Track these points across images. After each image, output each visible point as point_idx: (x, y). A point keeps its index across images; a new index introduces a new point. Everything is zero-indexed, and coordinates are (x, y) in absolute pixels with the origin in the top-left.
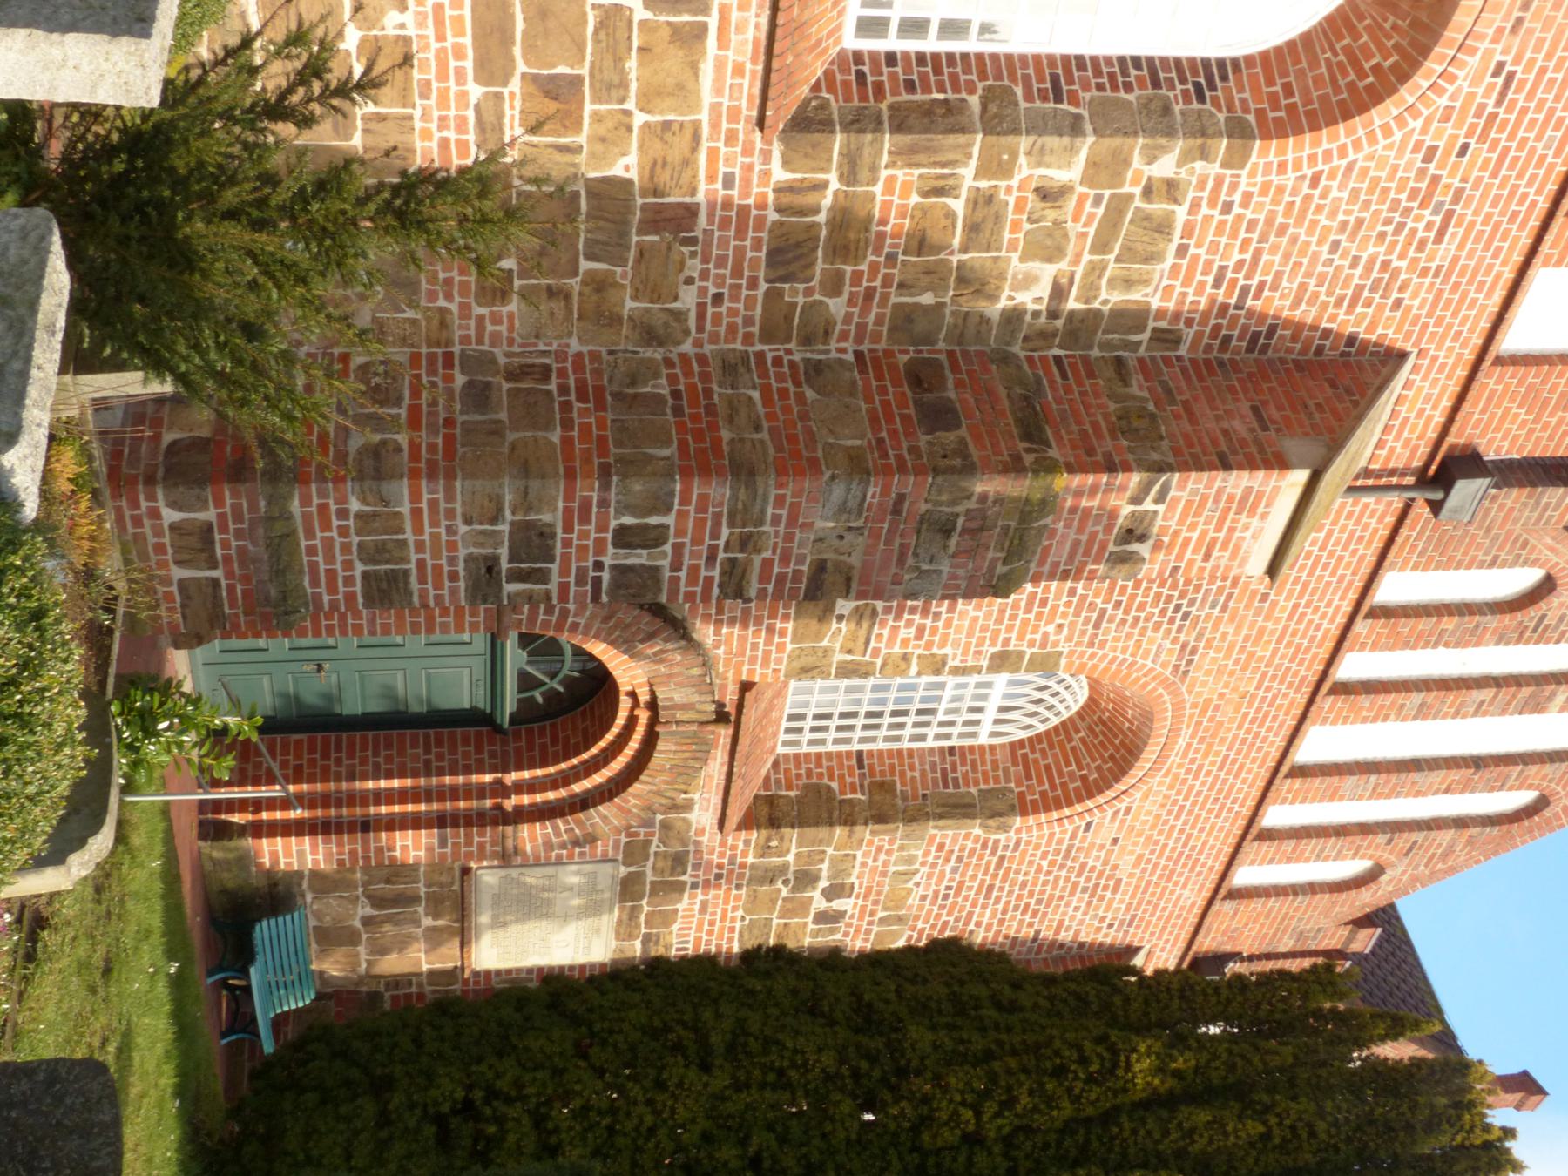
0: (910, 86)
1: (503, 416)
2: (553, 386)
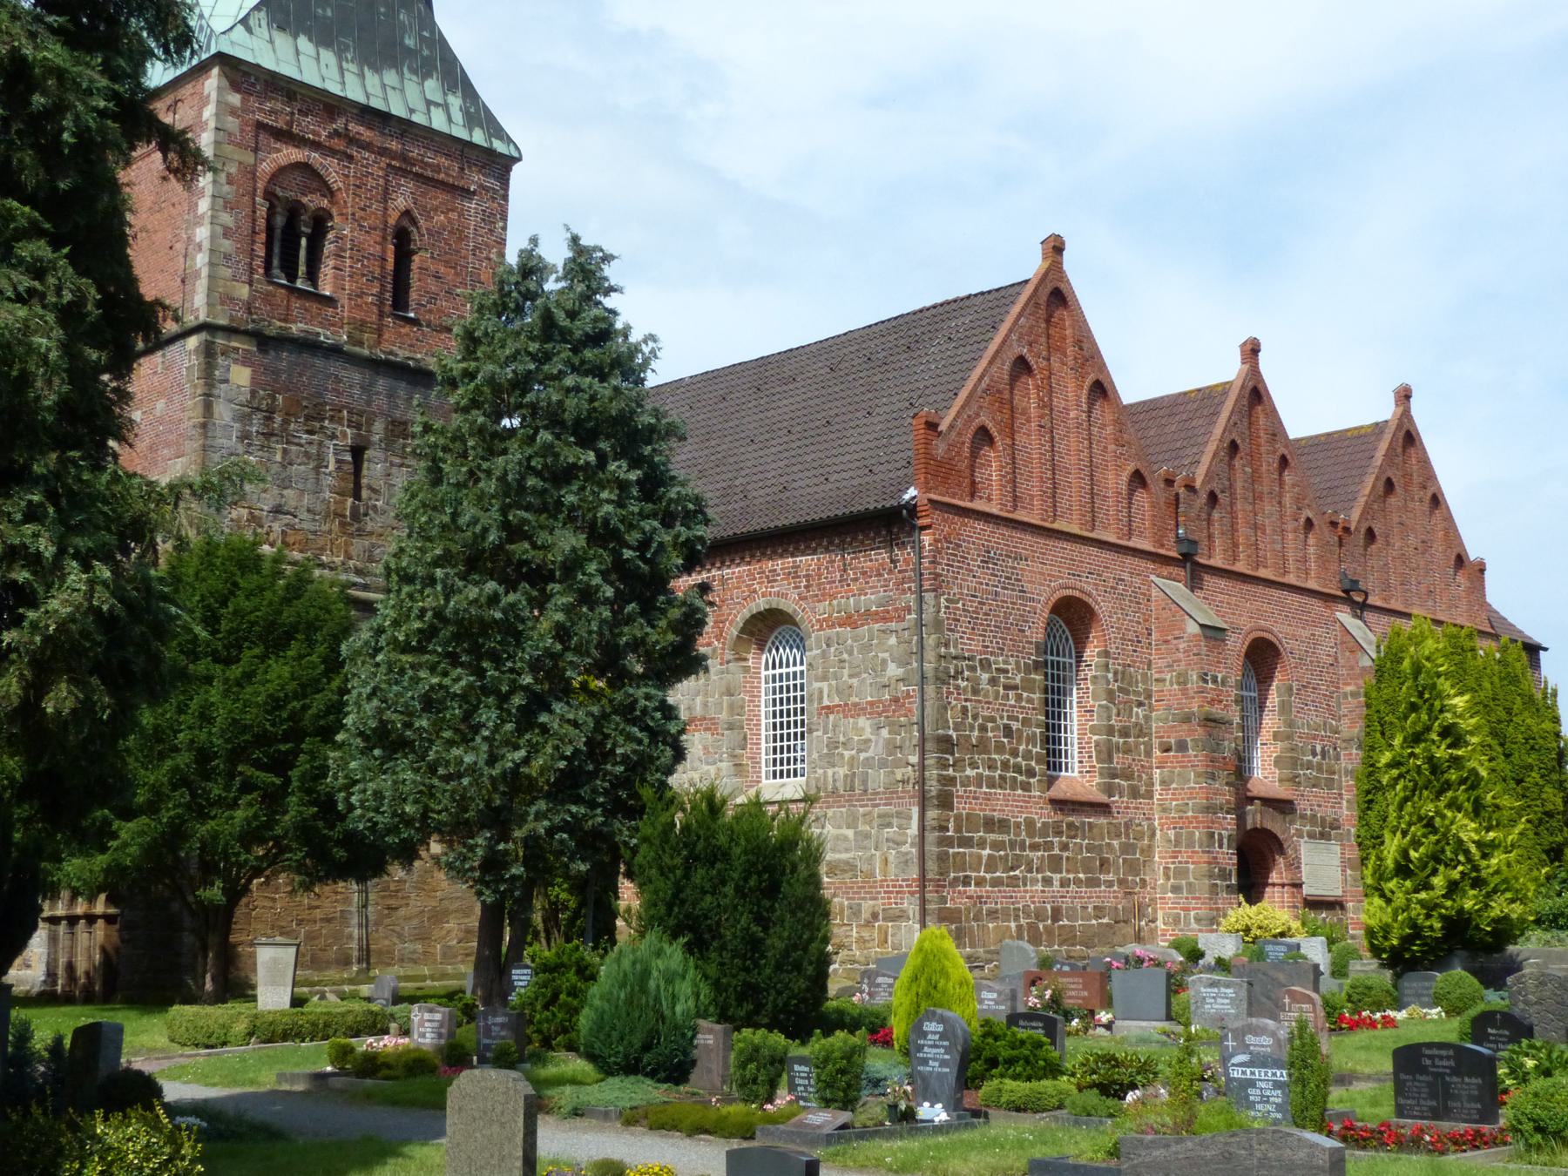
0: (1090, 757)
1: (1184, 882)
2: (1172, 866)
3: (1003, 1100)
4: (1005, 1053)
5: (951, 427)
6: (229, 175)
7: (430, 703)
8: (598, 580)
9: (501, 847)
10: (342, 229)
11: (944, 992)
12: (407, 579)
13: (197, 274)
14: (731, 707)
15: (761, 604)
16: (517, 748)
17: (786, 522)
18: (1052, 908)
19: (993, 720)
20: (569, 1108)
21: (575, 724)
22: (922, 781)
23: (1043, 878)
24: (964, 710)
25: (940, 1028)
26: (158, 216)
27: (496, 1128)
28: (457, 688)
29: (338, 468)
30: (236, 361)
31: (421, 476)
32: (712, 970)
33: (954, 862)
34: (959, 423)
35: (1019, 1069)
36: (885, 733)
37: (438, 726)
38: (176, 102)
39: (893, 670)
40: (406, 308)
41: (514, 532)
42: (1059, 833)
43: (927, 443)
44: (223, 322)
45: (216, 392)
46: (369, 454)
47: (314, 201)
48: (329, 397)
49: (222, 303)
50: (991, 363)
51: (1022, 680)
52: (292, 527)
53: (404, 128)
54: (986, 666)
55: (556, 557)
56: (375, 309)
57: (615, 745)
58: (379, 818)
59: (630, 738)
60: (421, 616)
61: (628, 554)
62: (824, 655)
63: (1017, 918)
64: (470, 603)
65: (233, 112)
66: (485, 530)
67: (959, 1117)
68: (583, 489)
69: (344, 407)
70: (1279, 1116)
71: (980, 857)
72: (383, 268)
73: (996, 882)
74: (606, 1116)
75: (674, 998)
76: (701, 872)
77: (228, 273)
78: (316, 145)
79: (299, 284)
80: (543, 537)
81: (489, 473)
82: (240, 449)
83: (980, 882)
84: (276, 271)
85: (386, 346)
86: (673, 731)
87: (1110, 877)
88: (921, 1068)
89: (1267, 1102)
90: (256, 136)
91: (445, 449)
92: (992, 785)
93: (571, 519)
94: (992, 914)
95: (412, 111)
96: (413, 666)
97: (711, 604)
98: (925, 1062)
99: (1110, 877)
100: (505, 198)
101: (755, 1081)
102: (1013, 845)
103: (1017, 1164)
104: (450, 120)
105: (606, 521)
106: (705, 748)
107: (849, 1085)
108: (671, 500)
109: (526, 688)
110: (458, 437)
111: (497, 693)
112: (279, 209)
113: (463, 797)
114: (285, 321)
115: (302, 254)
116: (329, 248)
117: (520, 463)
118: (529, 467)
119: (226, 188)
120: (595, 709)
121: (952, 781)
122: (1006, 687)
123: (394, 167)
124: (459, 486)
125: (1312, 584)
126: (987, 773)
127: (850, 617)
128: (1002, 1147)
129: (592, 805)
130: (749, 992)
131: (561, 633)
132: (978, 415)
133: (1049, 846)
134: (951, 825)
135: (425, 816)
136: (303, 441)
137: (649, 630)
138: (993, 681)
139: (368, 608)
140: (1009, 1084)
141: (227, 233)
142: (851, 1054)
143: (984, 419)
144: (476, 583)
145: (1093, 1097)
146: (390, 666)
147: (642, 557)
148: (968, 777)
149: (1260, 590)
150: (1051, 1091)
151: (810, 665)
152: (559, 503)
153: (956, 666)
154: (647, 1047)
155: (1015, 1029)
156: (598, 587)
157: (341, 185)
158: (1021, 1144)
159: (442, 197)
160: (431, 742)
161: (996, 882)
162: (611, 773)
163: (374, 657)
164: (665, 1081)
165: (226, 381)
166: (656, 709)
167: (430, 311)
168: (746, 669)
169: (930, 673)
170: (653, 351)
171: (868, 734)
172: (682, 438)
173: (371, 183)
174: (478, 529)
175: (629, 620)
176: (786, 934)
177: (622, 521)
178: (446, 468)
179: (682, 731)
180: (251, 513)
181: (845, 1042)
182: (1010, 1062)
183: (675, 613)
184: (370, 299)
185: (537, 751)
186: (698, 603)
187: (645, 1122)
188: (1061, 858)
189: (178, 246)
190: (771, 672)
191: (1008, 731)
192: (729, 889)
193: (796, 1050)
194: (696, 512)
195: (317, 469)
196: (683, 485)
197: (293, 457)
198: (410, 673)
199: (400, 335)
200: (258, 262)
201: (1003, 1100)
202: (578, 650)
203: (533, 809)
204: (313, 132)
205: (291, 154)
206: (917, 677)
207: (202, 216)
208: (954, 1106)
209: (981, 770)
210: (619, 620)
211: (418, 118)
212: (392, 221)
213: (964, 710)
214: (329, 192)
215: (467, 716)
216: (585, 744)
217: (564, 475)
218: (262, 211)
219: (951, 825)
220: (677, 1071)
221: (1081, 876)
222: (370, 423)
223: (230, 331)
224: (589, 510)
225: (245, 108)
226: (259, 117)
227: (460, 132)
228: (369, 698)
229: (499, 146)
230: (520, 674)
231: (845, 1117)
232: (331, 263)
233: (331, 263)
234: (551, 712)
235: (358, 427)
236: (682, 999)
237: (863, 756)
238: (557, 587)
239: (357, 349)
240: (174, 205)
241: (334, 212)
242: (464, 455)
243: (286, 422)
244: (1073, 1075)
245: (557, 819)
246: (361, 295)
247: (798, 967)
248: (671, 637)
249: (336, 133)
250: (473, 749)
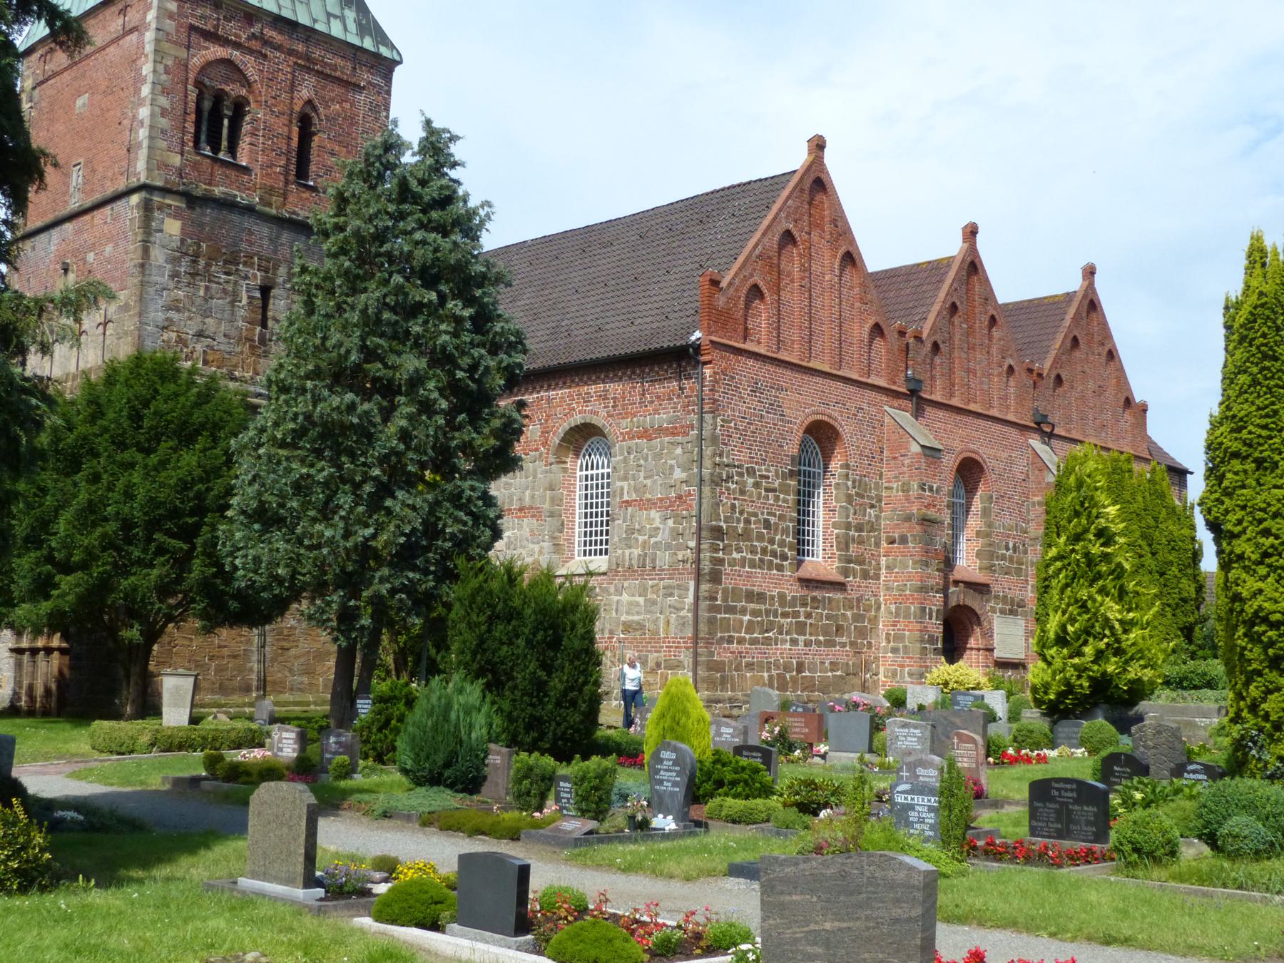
3: (723, 813)
4: (729, 776)
5: (730, 284)
6: (166, 66)
7: (300, 487)
8: (435, 395)
9: (352, 603)
10: (257, 113)
11: (684, 727)
12: (284, 389)
13: (139, 145)
14: (553, 499)
15: (578, 419)
16: (367, 526)
17: (599, 356)
18: (797, 663)
19: (755, 515)
20: (380, 811)
21: (413, 508)
22: (698, 561)
23: (791, 639)
24: (733, 507)
25: (673, 756)
26: (110, 97)
27: (285, 830)
28: (320, 477)
29: (250, 303)
30: (169, 215)
31: (299, 308)
32: (506, 705)
33: (721, 625)
34: (737, 281)
35: (739, 789)
36: (670, 523)
37: (305, 505)
38: (126, 7)
39: (679, 474)
40: (306, 178)
41: (370, 354)
42: (804, 605)
43: (711, 296)
44: (159, 183)
45: (152, 239)
46: (274, 292)
47: (234, 89)
48: (243, 245)
50: (764, 234)
51: (780, 484)
52: (211, 348)
53: (309, 34)
54: (751, 472)
55: (402, 376)
56: (282, 178)
57: (445, 526)
58: (257, 578)
59: (457, 520)
60: (294, 419)
61: (460, 374)
62: (625, 460)
63: (769, 669)
64: (333, 410)
65: (171, 16)
66: (348, 352)
67: (685, 827)
68: (426, 322)
69: (255, 254)
70: (931, 833)
71: (741, 622)
72: (288, 145)
73: (754, 642)
74: (408, 818)
75: (471, 726)
76: (501, 627)
77: (164, 144)
78: (237, 45)
79: (221, 156)
80: (392, 359)
81: (353, 307)
82: (171, 285)
83: (741, 641)
84: (203, 145)
85: (289, 207)
86: (492, 515)
87: (844, 639)
88: (657, 787)
89: (923, 822)
90: (189, 37)
91: (318, 287)
92: (753, 565)
93: (417, 345)
94: (750, 666)
95: (315, 21)
96: (287, 459)
97: (527, 416)
98: (661, 782)
99: (844, 639)
100: (389, 93)
101: (528, 793)
102: (768, 612)
103: (720, 867)
104: (345, 29)
105: (444, 348)
106: (532, 531)
107: (601, 799)
108: (496, 333)
109: (375, 479)
110: (328, 278)
111: (353, 482)
112: (206, 96)
113: (323, 564)
114: (210, 184)
115: (225, 132)
116: (246, 128)
117: (378, 300)
118: (386, 304)
119: (164, 77)
120: (430, 497)
121: (721, 561)
122: (767, 490)
123: (299, 65)
124: (327, 316)
125: (1011, 417)
126: (749, 556)
127: (646, 431)
128: (710, 853)
129: (426, 572)
130: (534, 723)
131: (405, 436)
132: (752, 276)
133: (796, 614)
134: (719, 597)
135: (295, 573)
136: (222, 281)
137: (474, 435)
138: (757, 485)
139: (254, 409)
140: (730, 801)
142: (602, 775)
143: (757, 279)
144: (339, 394)
145: (793, 813)
146: (270, 458)
147: (471, 378)
148: (735, 559)
149: (970, 420)
150: (761, 807)
151: (615, 468)
152: (407, 333)
153: (728, 472)
154: (447, 765)
155: (738, 758)
156: (435, 401)
157: (257, 78)
158: (726, 850)
159: (337, 90)
160: (299, 518)
161: (754, 642)
162: (442, 548)
163: (256, 450)
164: (462, 791)
165: (161, 231)
166: (479, 498)
168: (565, 470)
169: (706, 477)
170: (488, 215)
171: (657, 523)
172: (509, 285)
173: (281, 77)
174: (343, 351)
175: (459, 428)
176: (565, 678)
177: (456, 348)
178: (318, 301)
179: (500, 517)
180: (179, 336)
181: (599, 765)
182: (733, 783)
183: (496, 423)
184: (278, 170)
185: (383, 529)
186: (515, 415)
187: (436, 825)
188: (806, 624)
189: (126, 122)
190: (584, 473)
191: (767, 524)
192: (521, 642)
193: (563, 770)
194: (517, 343)
195: (233, 303)
196: (507, 321)
197: (214, 293)
198: (285, 464)
199: (301, 199)
200: (189, 137)
201: (723, 813)
202: (417, 450)
203: (378, 574)
204: (236, 35)
206: (697, 480)
207: (144, 99)
208: (682, 817)
209: (744, 554)
210: (452, 425)
211: (320, 27)
212: (297, 108)
213: (733, 507)
214: (247, 83)
215: (329, 499)
216: (421, 524)
217: (415, 310)
218: (193, 96)
219: (719, 597)
220: (471, 784)
221: (821, 638)
222: (276, 267)
223: (165, 191)
224: (431, 339)
225: (180, 13)
226: (192, 21)
227: (353, 39)
228: (250, 484)
229: (384, 51)
230: (370, 468)
231: (592, 824)
233: (248, 139)
234: (394, 498)
235: (267, 271)
236: (477, 727)
237: (653, 540)
238: (403, 399)
239: (267, 209)
240: (122, 89)
241: (251, 98)
242: (333, 292)
243: (208, 265)
244: (781, 795)
245: (397, 583)
246: (272, 166)
247: (574, 703)
248: (492, 442)
249: (253, 36)
250: (332, 525)
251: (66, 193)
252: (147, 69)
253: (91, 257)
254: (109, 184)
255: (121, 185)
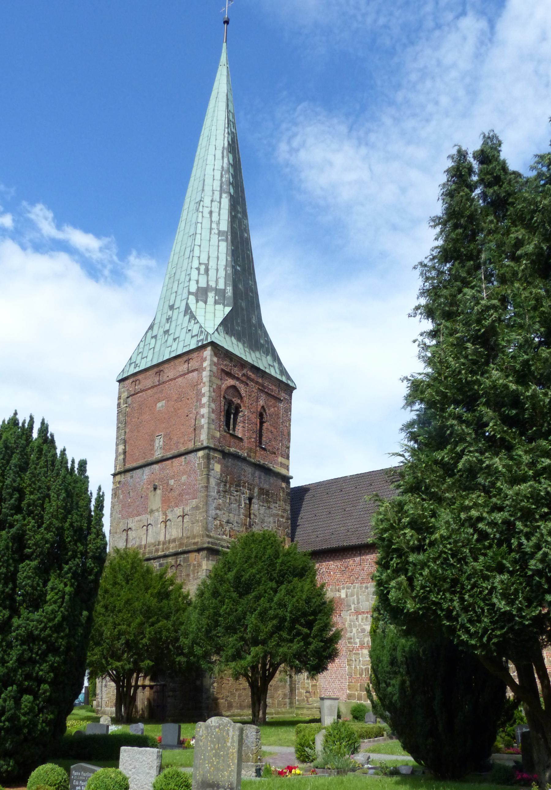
6: (214, 388)
13: (202, 427)
26: (180, 403)
44: (212, 446)
47: (236, 401)
48: (242, 477)
49: (212, 439)
65: (215, 364)
69: (247, 482)
78: (238, 379)
114: (229, 447)
115: (232, 421)
116: (240, 419)
119: (213, 394)
141: (213, 412)
165: (213, 470)
167: (269, 446)
173: (253, 395)
184: (253, 440)
199: (261, 454)
205: (231, 382)
207: (204, 404)
214: (241, 398)
222: (254, 489)
223: (215, 450)
226: (222, 367)
232: (241, 425)
233: (241, 425)
235: (251, 491)
240: (188, 399)
241: (242, 405)
243: (230, 487)
246: (250, 438)
249: (244, 375)
251: (152, 449)
252: (205, 390)
253: (172, 482)
254: (181, 445)
255: (191, 446)
